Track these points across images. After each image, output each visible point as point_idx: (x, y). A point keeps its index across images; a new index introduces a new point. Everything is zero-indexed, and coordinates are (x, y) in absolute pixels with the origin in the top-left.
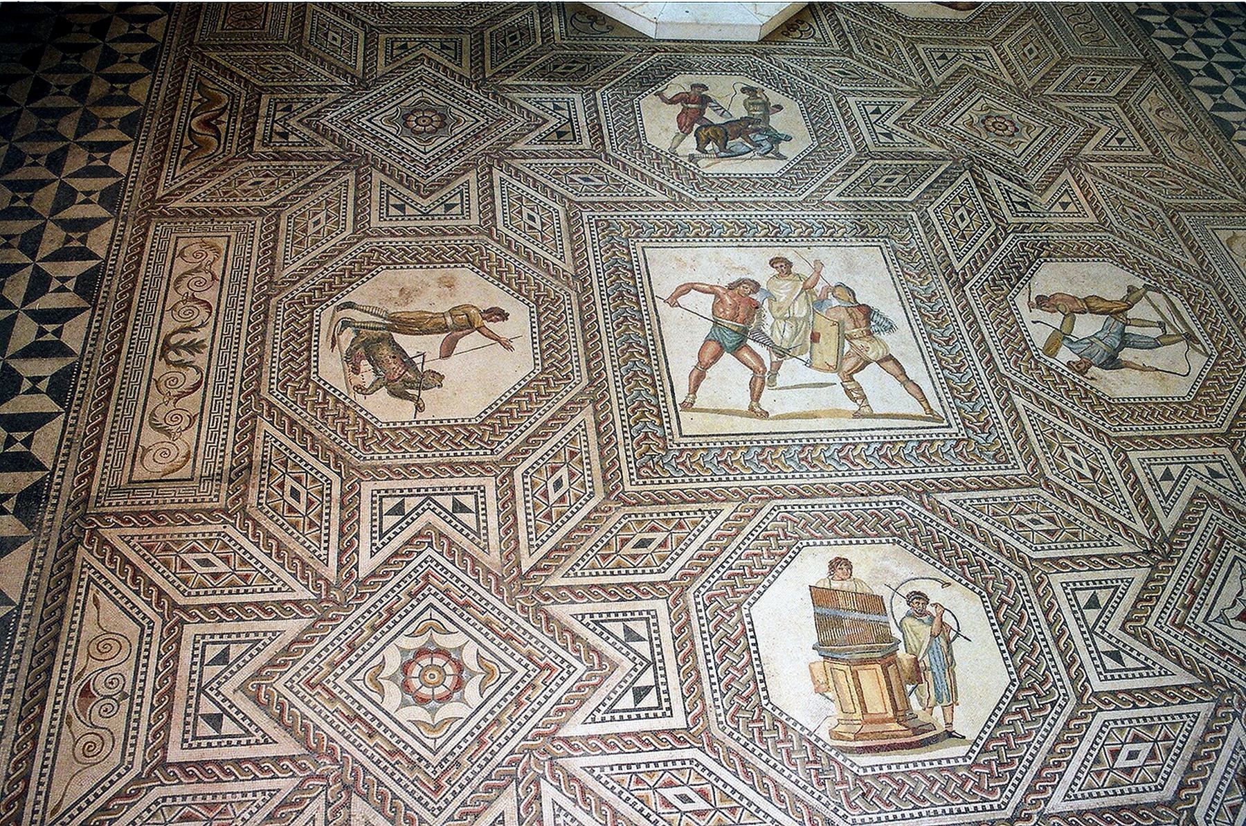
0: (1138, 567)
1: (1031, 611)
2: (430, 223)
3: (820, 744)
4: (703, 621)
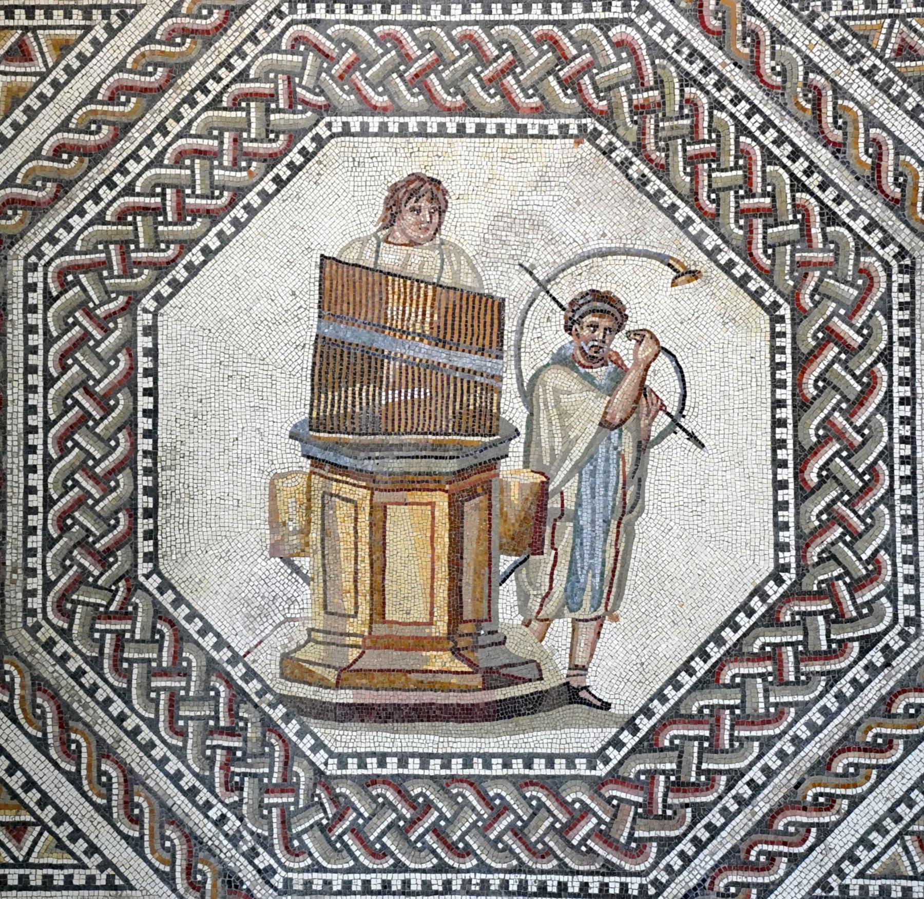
3: (252, 688)
4: (37, 340)
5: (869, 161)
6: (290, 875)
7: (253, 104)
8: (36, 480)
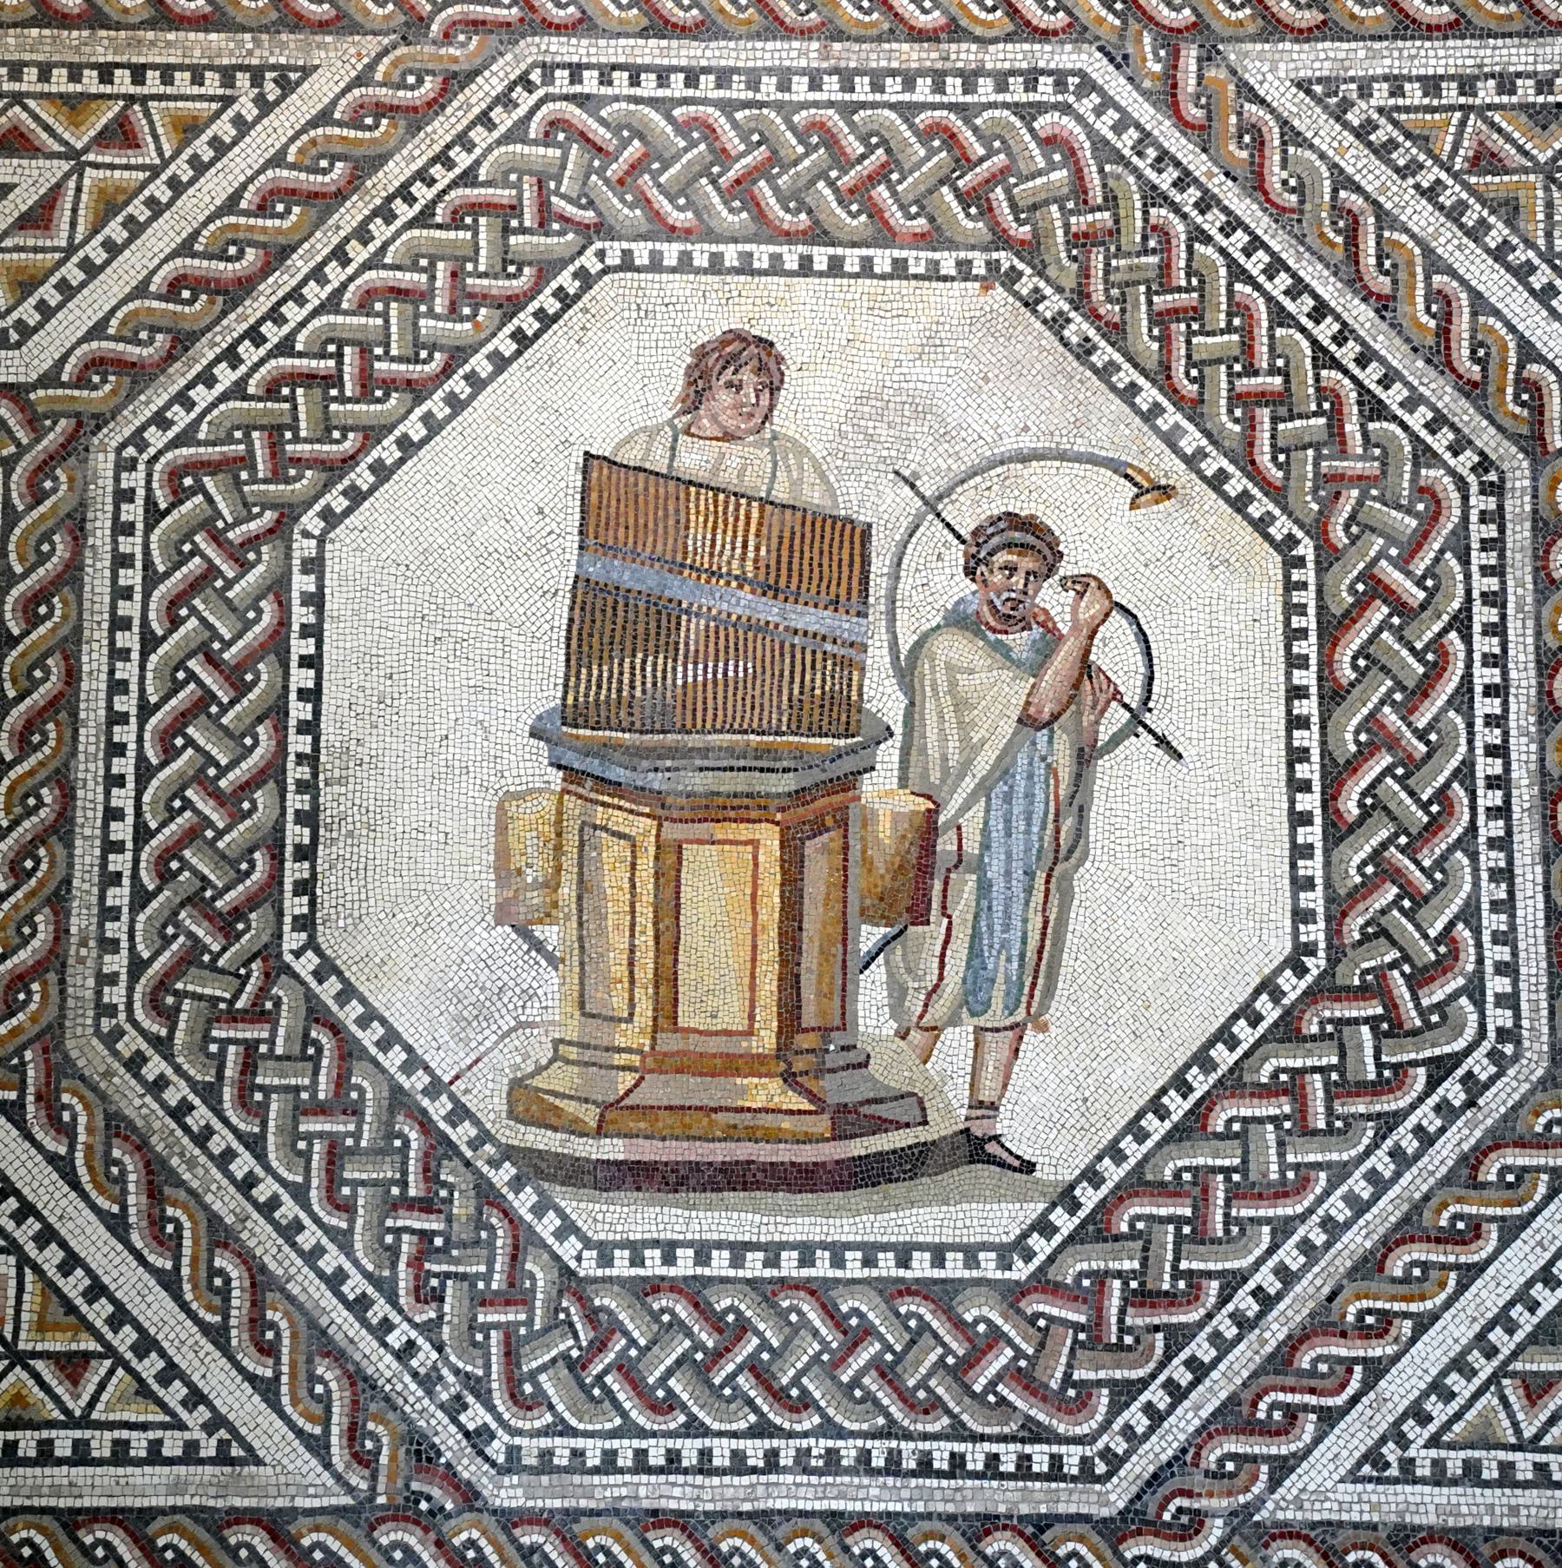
1: (1485, 645)
3: (462, 1134)
4: (132, 577)
5: (1432, 324)
6: (517, 1441)
7: (482, 220)
8: (123, 798)
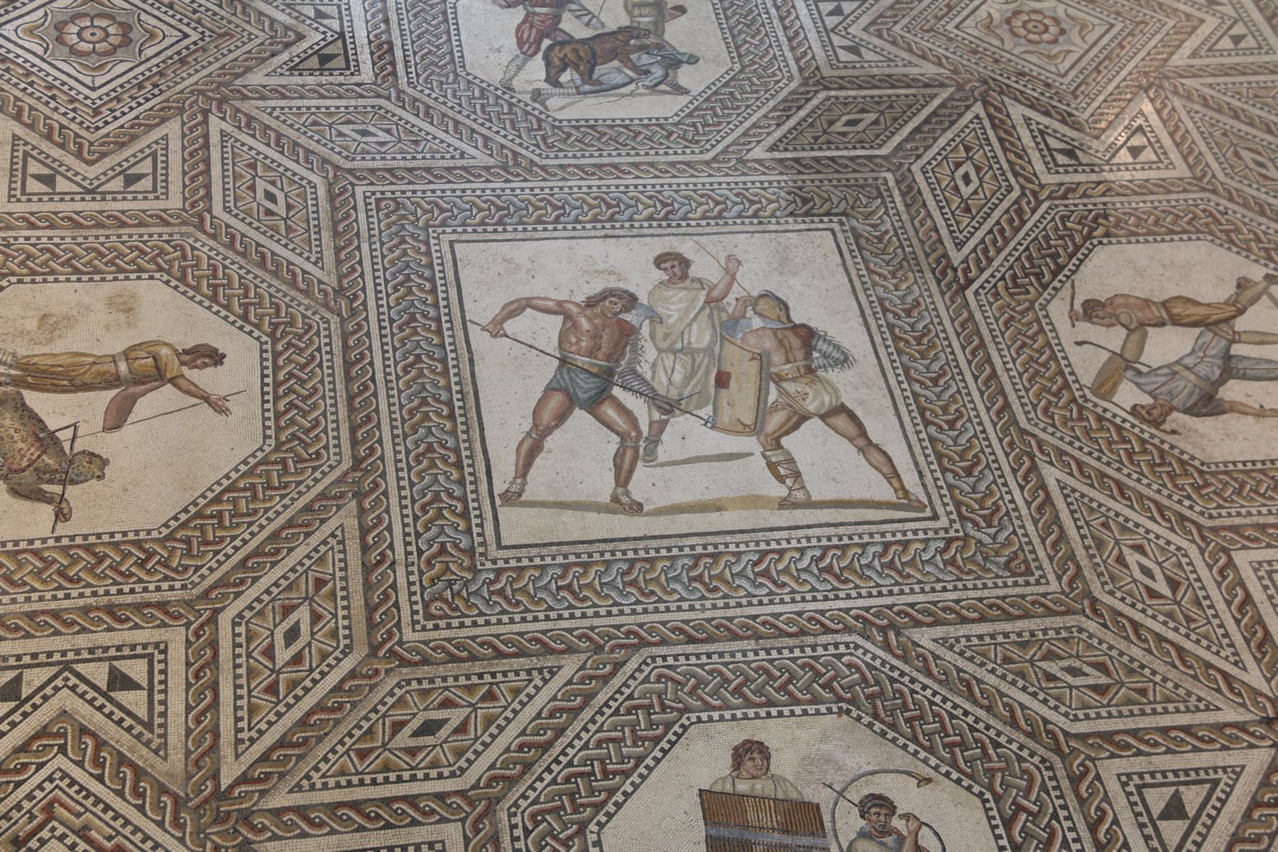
0: (1252, 746)
2: (96, 206)
